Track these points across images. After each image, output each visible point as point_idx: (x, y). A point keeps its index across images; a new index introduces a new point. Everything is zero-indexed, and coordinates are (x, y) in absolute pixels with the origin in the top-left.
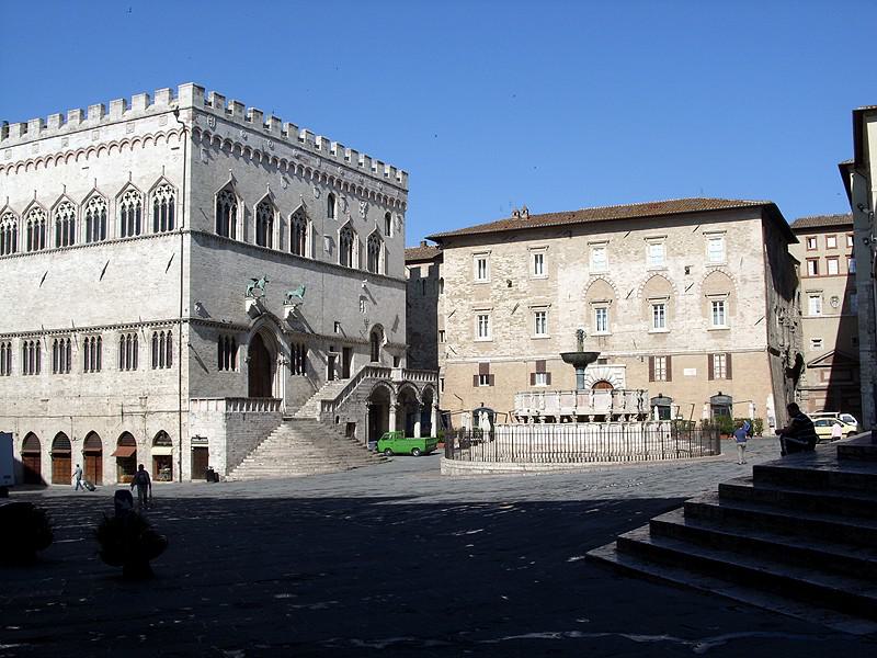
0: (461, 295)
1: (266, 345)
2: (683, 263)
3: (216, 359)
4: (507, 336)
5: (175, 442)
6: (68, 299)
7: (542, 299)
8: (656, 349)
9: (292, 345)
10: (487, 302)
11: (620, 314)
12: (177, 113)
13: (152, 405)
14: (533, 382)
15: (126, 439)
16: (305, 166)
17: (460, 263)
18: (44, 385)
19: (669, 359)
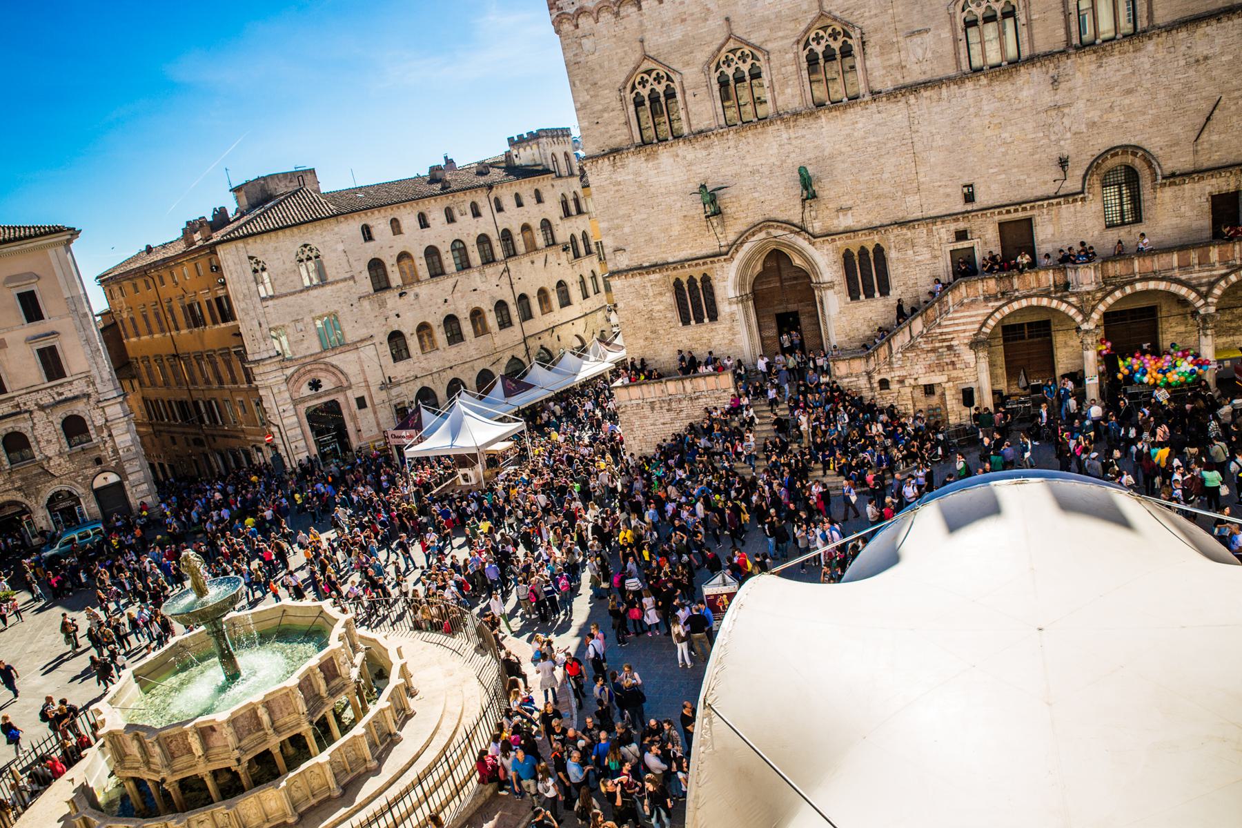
1: (798, 261)
3: (674, 315)
9: (847, 256)
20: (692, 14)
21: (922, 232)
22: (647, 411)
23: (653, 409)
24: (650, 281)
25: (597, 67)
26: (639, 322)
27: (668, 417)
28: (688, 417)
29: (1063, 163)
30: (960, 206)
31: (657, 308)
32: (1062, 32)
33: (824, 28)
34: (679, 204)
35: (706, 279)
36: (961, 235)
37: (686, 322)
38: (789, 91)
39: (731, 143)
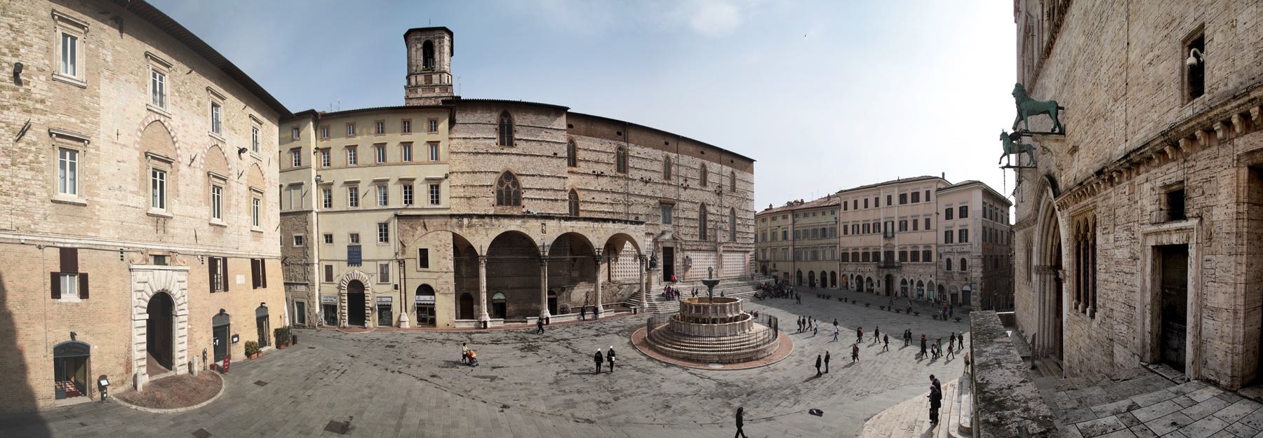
7: (72, 124)
11: (182, 188)
14: (56, 293)
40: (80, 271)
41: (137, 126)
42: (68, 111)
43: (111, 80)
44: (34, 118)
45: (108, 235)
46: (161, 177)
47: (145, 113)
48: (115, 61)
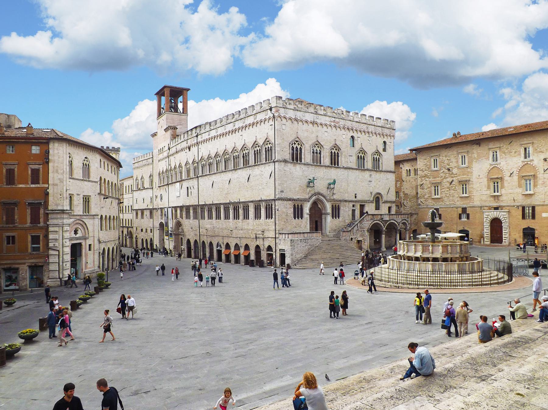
0: (426, 176)
1: (319, 206)
2: (542, 156)
3: (292, 215)
4: (448, 195)
5: (274, 251)
6: (237, 189)
7: (464, 177)
8: (527, 202)
9: (332, 206)
10: (438, 180)
12: (271, 109)
13: (266, 234)
15: (258, 247)
16: (337, 125)
17: (425, 161)
18: (231, 224)
19: (533, 208)
20: (309, 131)
21: (347, 203)
22: (299, 242)
23: (301, 241)
24: (289, 203)
25: (285, 134)
26: (284, 216)
27: (305, 244)
28: (310, 245)
29: (371, 193)
30: (354, 199)
31: (289, 212)
32: (371, 165)
33: (335, 147)
34: (299, 182)
35: (301, 206)
36: (353, 206)
37: (295, 218)
38: (327, 159)
39: (313, 168)
40: (467, 213)
41: (486, 171)
42: (463, 175)
43: (476, 162)
44: (454, 179)
45: (477, 203)
46: (497, 183)
47: (489, 166)
48: (477, 156)
